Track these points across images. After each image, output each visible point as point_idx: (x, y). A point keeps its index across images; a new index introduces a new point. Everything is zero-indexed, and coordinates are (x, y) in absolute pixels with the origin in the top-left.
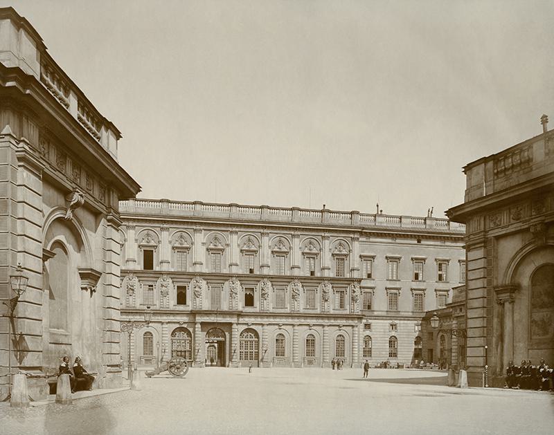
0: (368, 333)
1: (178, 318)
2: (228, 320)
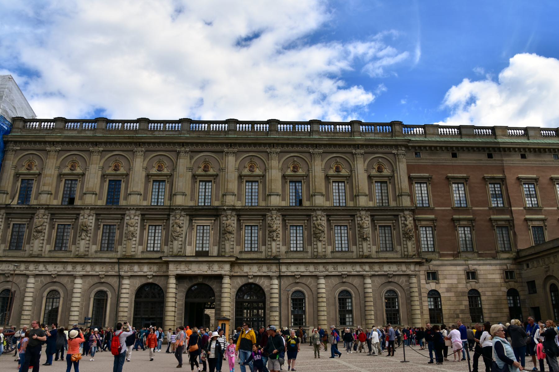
0: (432, 286)
1: (146, 268)
2: (216, 270)
